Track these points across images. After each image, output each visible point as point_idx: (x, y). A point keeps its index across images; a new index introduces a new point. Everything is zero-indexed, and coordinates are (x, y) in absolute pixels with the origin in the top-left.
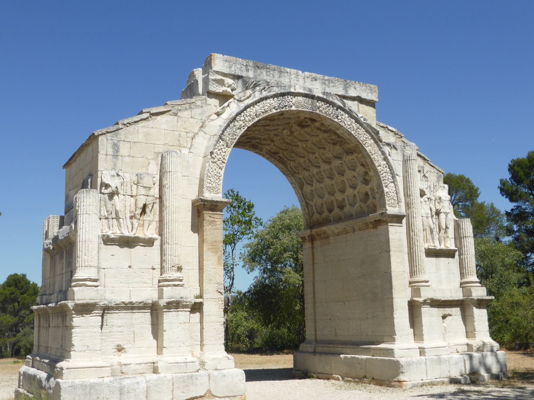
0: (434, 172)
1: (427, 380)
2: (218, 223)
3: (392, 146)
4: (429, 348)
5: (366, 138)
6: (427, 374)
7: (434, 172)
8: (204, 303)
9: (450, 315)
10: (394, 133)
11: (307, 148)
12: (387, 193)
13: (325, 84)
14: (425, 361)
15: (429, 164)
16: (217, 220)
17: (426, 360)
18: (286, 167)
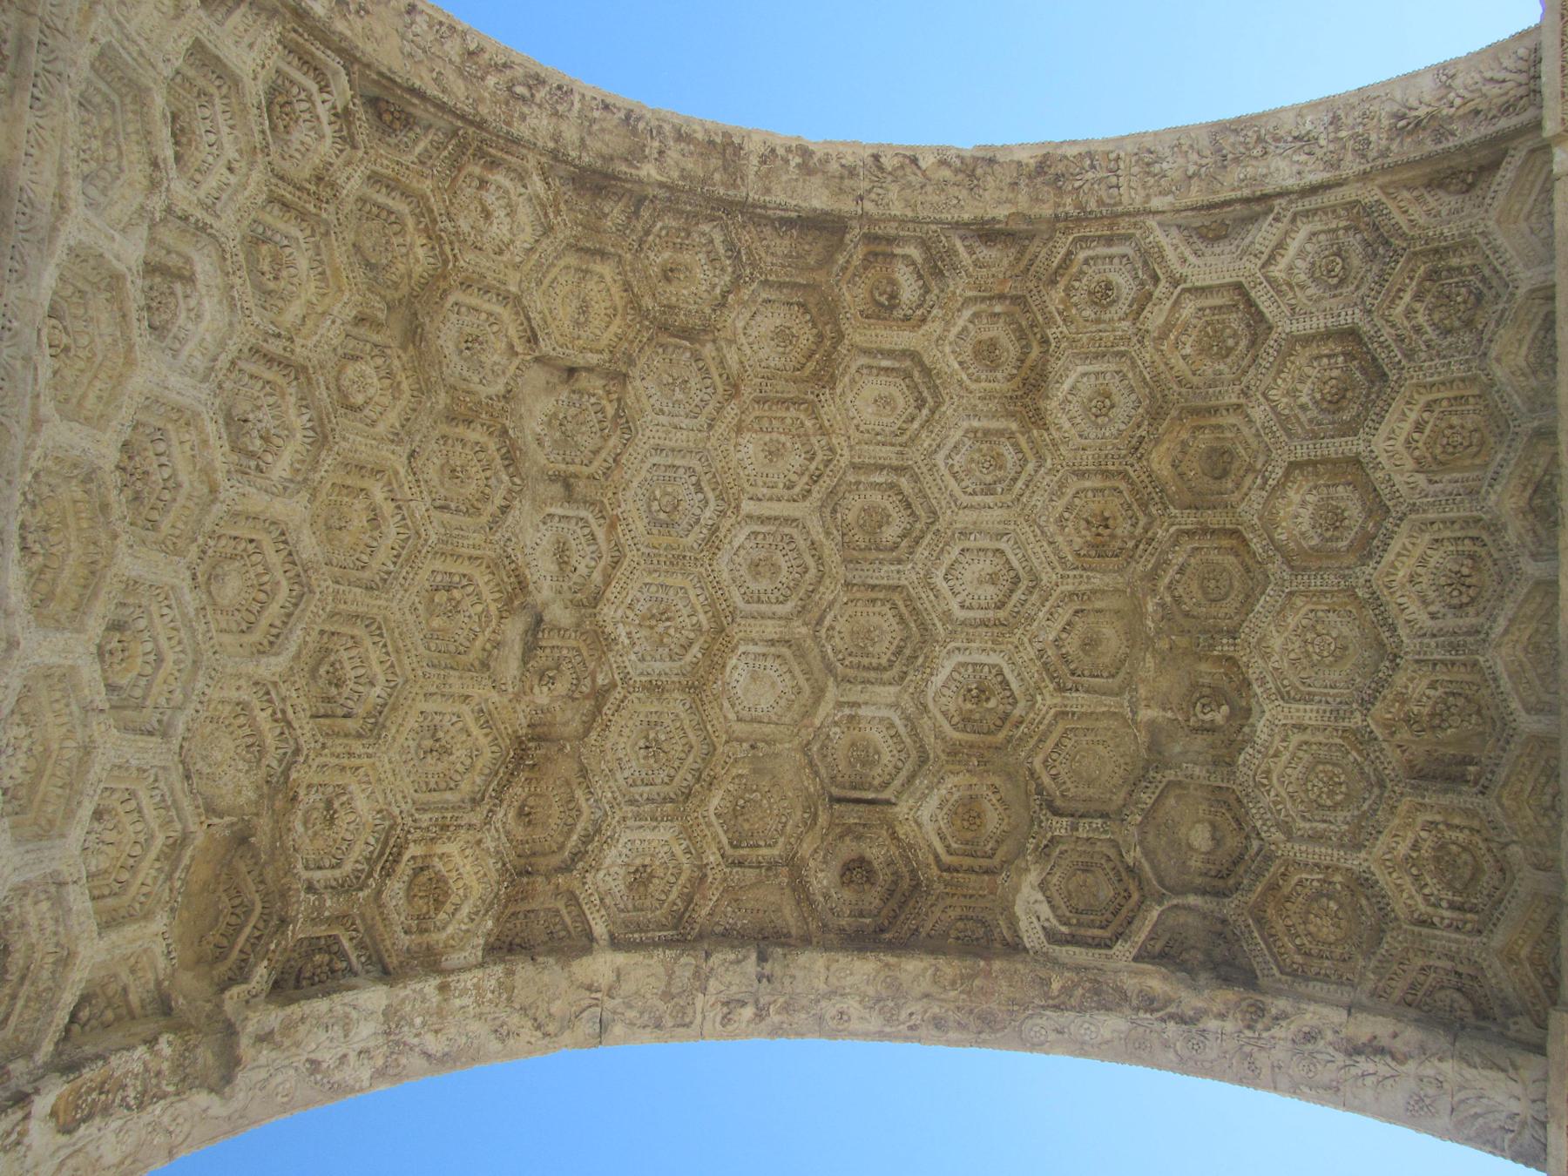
11: (349, 482)
18: (356, 60)
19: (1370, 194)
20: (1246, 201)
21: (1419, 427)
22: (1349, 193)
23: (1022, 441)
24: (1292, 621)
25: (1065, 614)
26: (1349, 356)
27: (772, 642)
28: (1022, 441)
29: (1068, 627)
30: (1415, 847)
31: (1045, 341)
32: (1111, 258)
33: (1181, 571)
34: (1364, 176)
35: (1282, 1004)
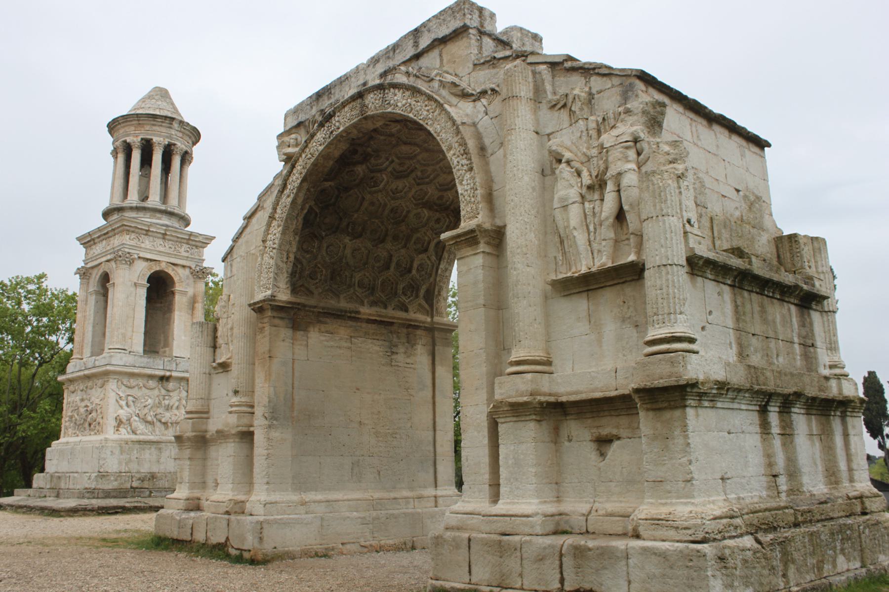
0: (613, 86)
1: (469, 584)
2: (266, 329)
3: (489, 92)
4: (490, 516)
5: (428, 111)
6: (470, 572)
7: (613, 86)
8: (256, 432)
9: (619, 438)
10: (511, 58)
12: (462, 194)
13: (389, 58)
14: (466, 542)
15: (598, 74)
16: (265, 325)
17: (469, 540)
19: (432, 279)
20: (441, 256)
21: (390, 280)
22: (433, 275)
23: (420, 201)
24: (363, 249)
25: (383, 203)
26: (405, 268)
27: (416, 155)
28: (420, 201)
29: (378, 200)
30: (319, 268)
31: (437, 211)
32: (444, 224)
33: (380, 227)
34: (435, 280)
35: (297, 238)
